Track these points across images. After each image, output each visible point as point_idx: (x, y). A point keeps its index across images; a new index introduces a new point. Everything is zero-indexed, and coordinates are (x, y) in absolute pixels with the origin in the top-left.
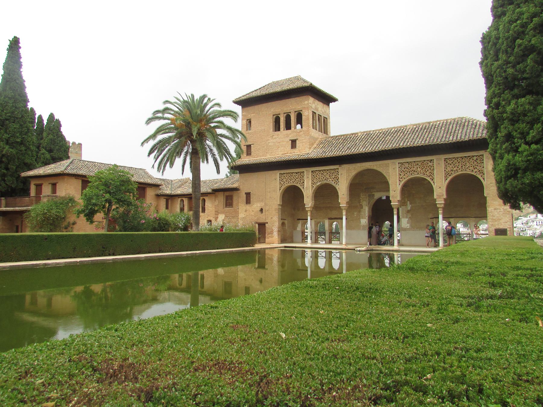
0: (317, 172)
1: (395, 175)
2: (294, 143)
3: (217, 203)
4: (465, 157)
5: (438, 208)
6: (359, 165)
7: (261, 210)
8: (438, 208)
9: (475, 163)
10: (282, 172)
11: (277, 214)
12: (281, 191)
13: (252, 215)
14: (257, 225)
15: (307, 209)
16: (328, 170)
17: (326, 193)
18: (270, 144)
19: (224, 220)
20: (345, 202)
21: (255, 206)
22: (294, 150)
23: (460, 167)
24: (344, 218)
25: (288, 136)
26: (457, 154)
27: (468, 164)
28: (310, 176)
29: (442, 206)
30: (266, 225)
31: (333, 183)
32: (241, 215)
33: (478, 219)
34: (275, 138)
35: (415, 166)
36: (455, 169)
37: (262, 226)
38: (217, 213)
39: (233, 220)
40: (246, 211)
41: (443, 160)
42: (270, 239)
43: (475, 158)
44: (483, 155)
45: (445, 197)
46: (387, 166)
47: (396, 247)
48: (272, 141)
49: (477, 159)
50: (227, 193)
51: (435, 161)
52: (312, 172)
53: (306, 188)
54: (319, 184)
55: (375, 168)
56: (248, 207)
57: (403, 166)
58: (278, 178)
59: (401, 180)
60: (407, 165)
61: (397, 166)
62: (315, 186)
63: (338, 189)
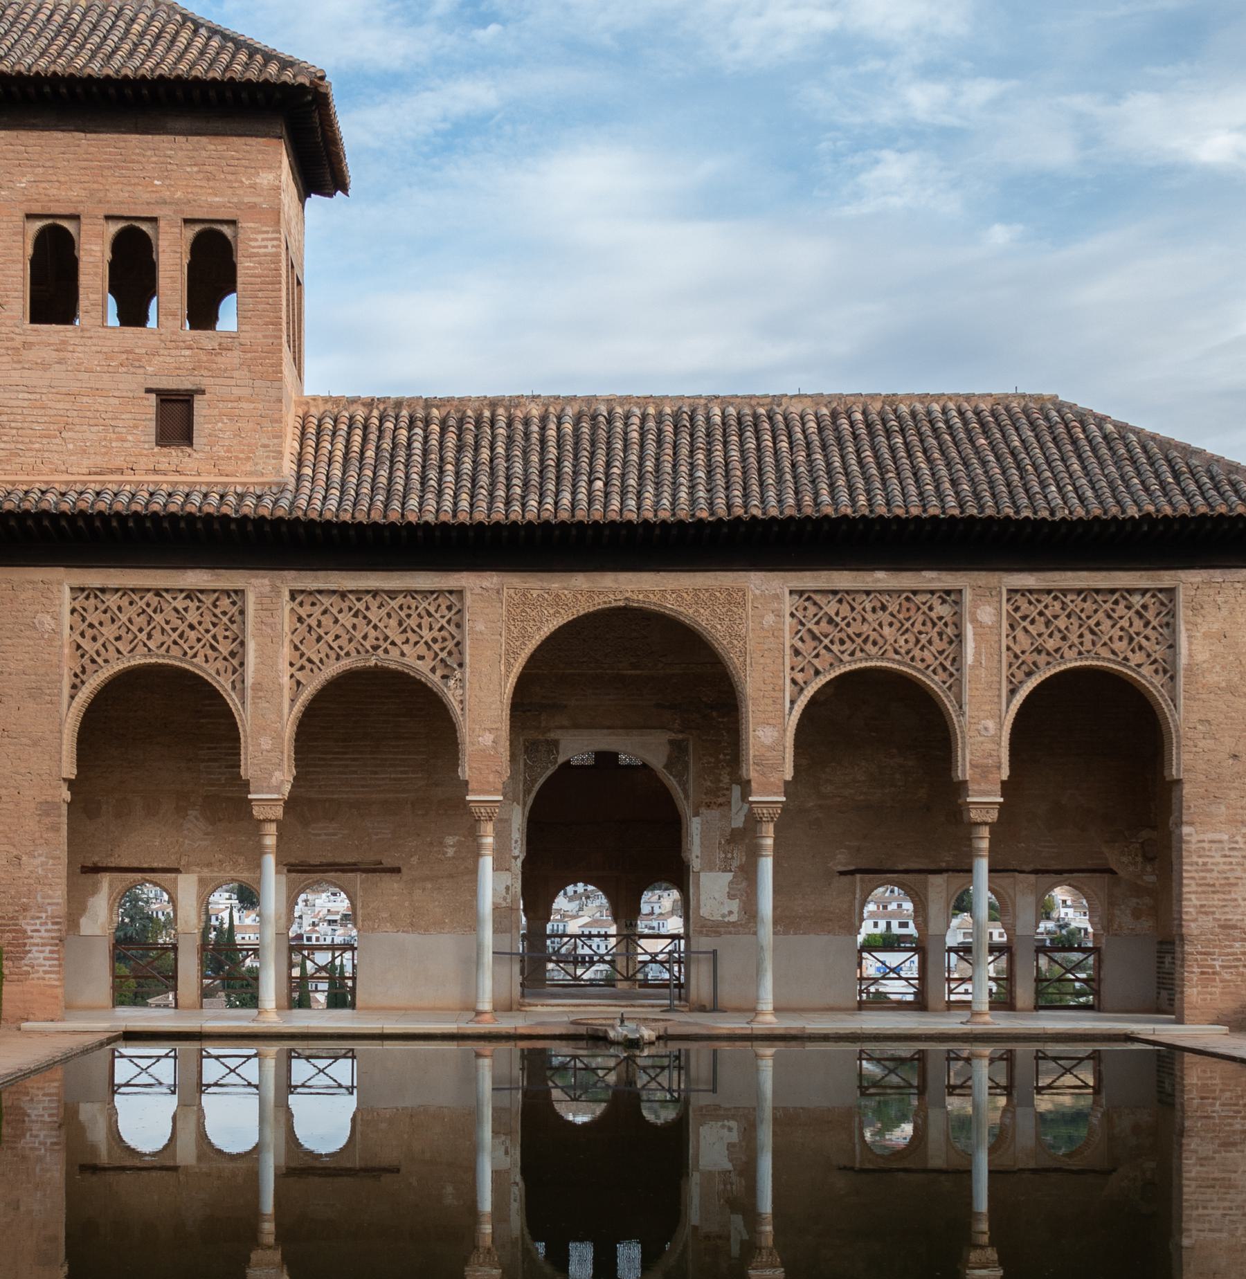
0: (326, 601)
2: (175, 415)
4: (1097, 591)
6: (580, 581)
9: (1138, 624)
10: (94, 578)
12: (85, 694)
15: (258, 812)
16: (392, 594)
17: (376, 727)
22: (174, 455)
23: (1074, 638)
24: (487, 863)
25: (132, 360)
26: (1069, 574)
27: (1107, 623)
28: (286, 620)
29: (993, 816)
31: (423, 668)
33: (1046, 879)
34: (45, 366)
35: (870, 616)
36: (1051, 644)
41: (1005, 597)
43: (1137, 600)
44: (1171, 592)
45: (1005, 774)
46: (736, 599)
47: (768, 1021)
48: (15, 376)
49: (1145, 607)
51: (968, 596)
52: (293, 595)
53: (257, 687)
54: (333, 669)
55: (670, 605)
57: (812, 610)
58: (67, 619)
59: (800, 677)
60: (831, 608)
61: (788, 603)
62: (313, 684)
63: (455, 706)
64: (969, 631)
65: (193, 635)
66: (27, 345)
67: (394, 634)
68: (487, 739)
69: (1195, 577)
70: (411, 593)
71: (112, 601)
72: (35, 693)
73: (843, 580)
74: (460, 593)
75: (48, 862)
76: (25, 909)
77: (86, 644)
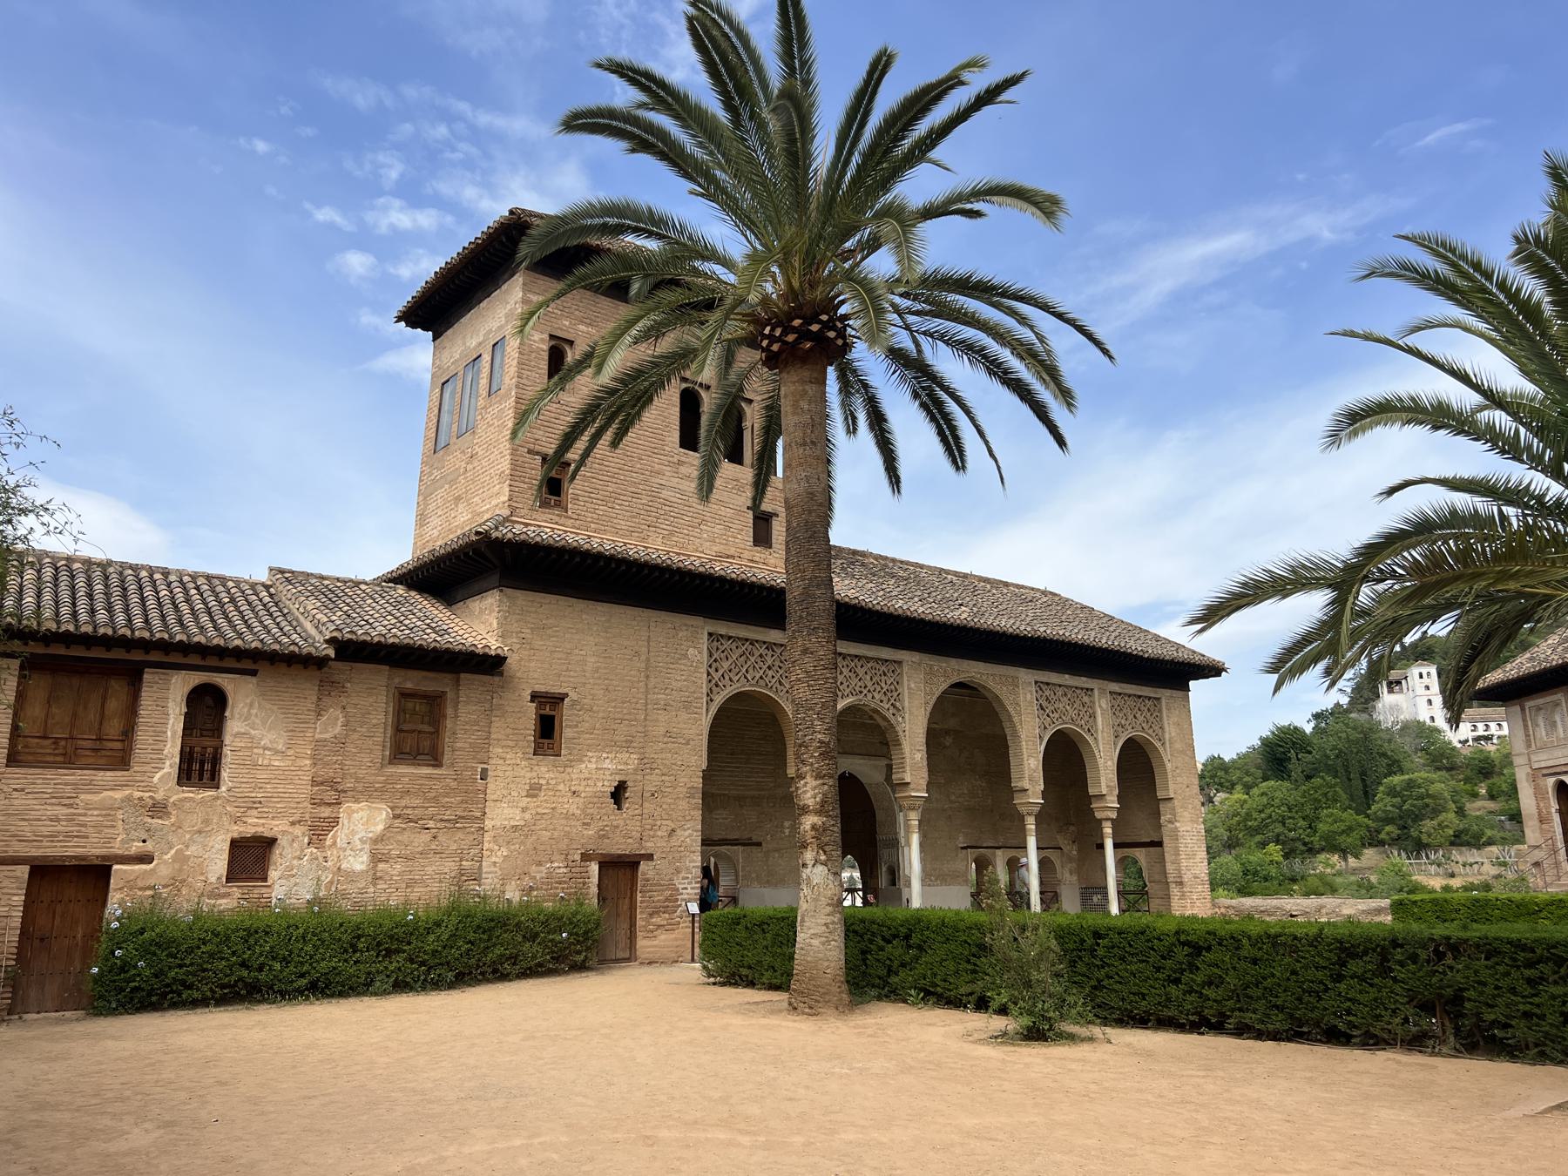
1: (1029, 713)
3: (331, 725)
5: (1100, 821)
6: (954, 663)
7: (618, 794)
8: (1100, 821)
10: (722, 628)
11: (698, 814)
13: (568, 816)
14: (594, 868)
16: (868, 659)
18: (665, 494)
19: (375, 841)
20: (924, 783)
21: (588, 766)
22: (759, 554)
30: (643, 866)
32: (503, 813)
37: (620, 870)
38: (331, 793)
39: (451, 842)
40: (534, 790)
42: (663, 938)
50: (413, 680)
51: (1096, 692)
56: (545, 770)
64: (1099, 711)
65: (770, 673)
66: (680, 463)
67: (869, 684)
68: (918, 756)
69: (1168, 692)
70: (877, 660)
71: (727, 644)
72: (687, 705)
73: (1054, 678)
74: (900, 663)
75: (690, 835)
76: (678, 871)
77: (712, 671)
